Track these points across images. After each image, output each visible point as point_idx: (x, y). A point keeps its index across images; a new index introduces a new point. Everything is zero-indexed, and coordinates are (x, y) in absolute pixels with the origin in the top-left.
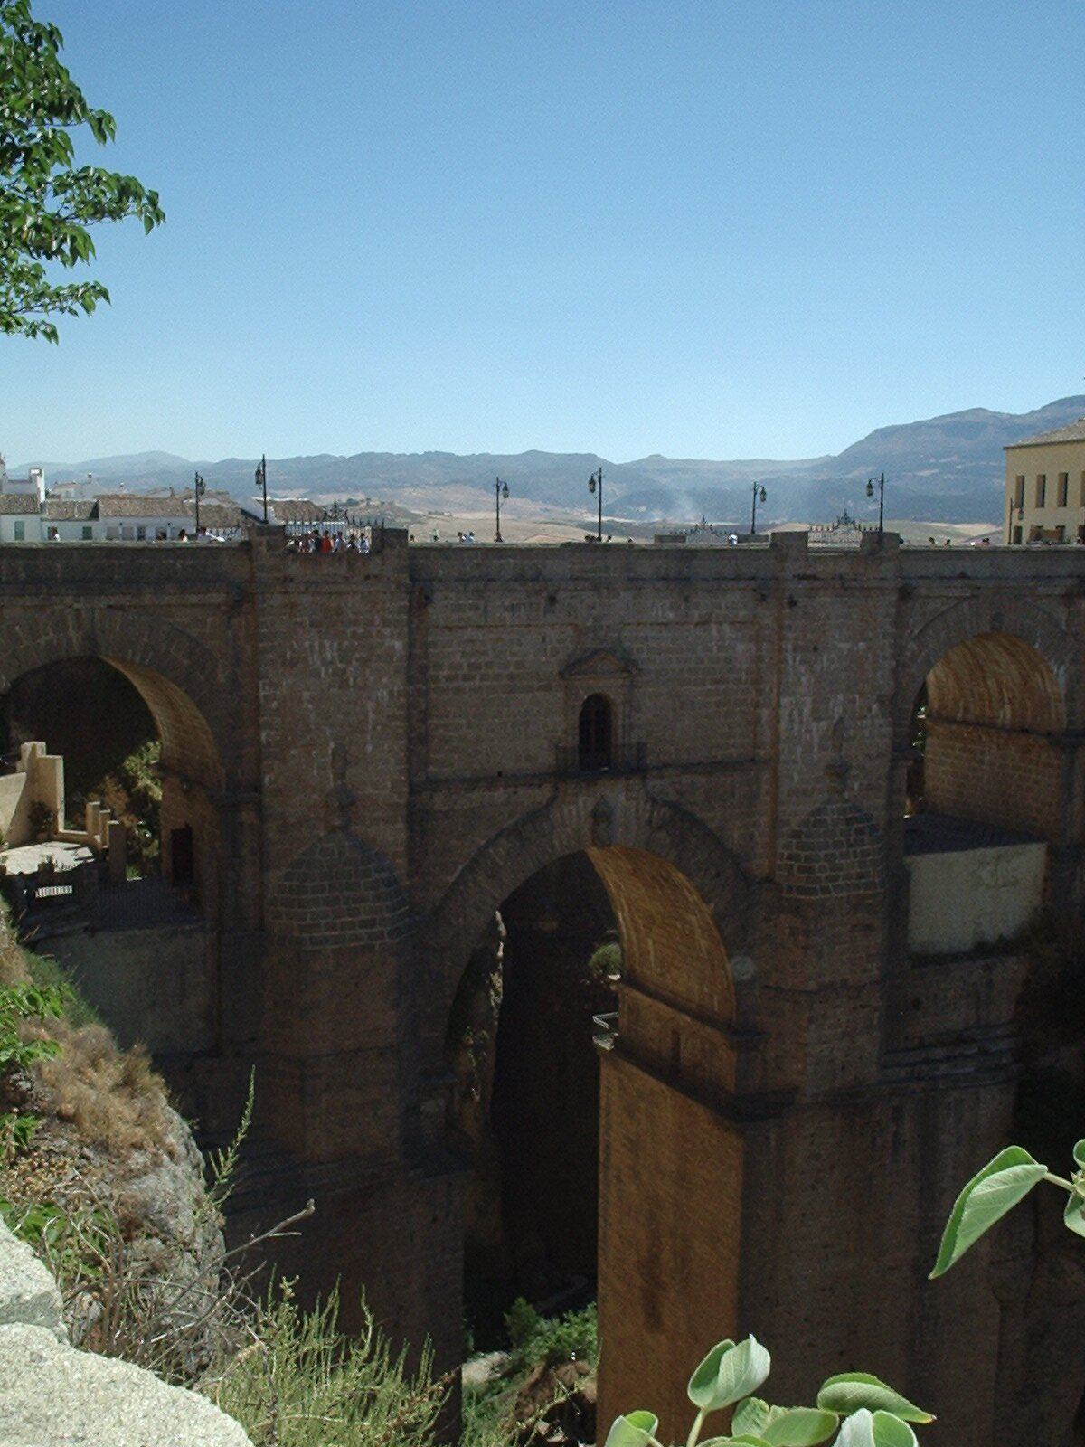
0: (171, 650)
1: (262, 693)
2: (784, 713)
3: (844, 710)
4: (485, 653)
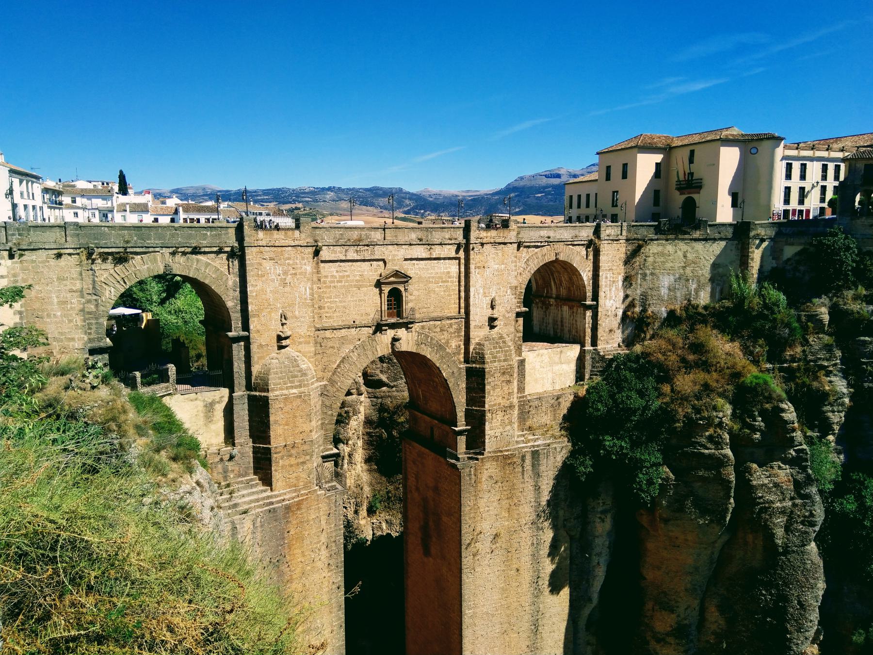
0: (207, 271)
2: (472, 294)
3: (497, 293)
4: (345, 271)
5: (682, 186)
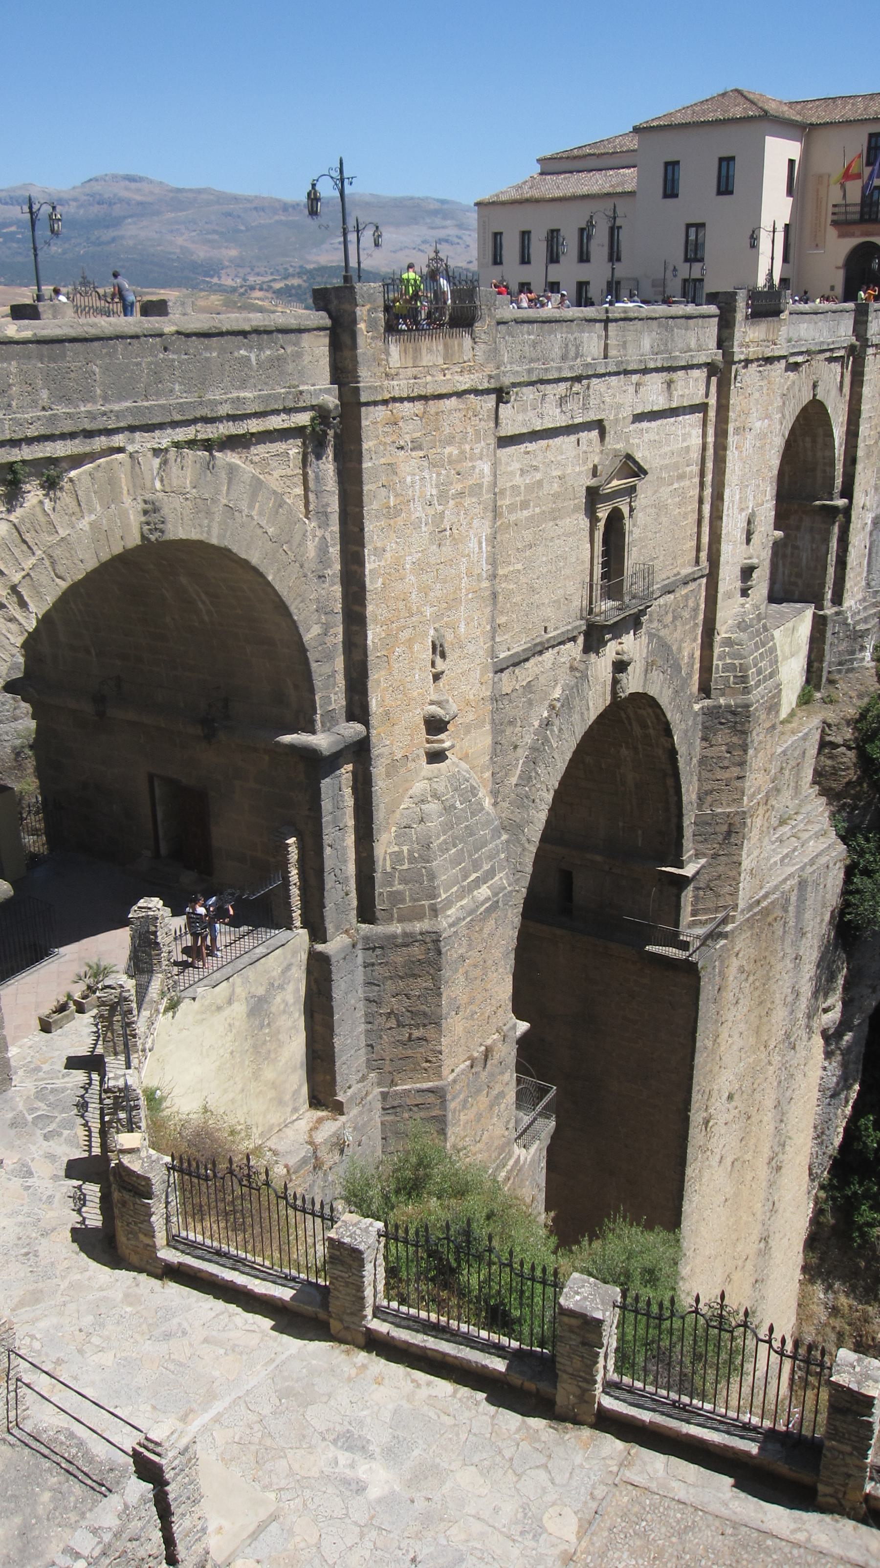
0: (254, 513)
1: (368, 567)
4: (536, 469)
5: (849, 217)
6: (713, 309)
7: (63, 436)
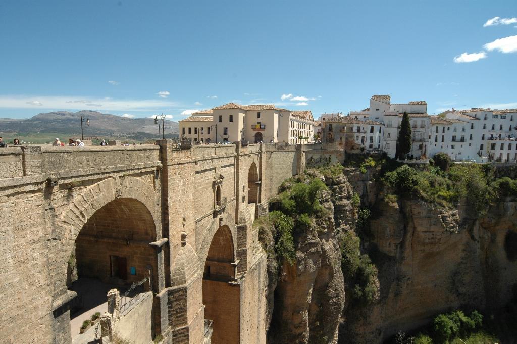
1: (169, 202)
6: (235, 145)
7: (97, 174)
